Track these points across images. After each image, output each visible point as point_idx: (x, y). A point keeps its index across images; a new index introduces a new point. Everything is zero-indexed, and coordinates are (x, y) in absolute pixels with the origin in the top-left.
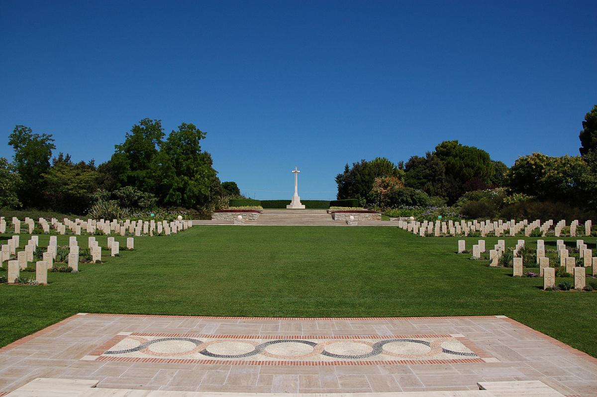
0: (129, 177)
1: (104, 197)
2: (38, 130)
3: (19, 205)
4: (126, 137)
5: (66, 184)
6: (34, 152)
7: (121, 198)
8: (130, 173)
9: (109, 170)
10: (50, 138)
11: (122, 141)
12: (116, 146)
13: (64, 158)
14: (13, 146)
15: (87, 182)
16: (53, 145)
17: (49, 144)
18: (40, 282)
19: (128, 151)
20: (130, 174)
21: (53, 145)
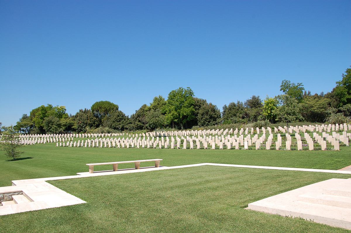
0: (347, 99)
1: (334, 112)
2: (294, 81)
3: (302, 119)
4: (342, 76)
5: (312, 107)
6: (295, 93)
7: (344, 111)
8: (348, 96)
9: (333, 97)
10: (301, 84)
11: (341, 79)
12: (337, 83)
13: (307, 93)
14: (282, 91)
15: (323, 105)
16: (303, 88)
17: (301, 87)
18: (336, 150)
19: (345, 84)
20: (348, 97)
21: (303, 88)
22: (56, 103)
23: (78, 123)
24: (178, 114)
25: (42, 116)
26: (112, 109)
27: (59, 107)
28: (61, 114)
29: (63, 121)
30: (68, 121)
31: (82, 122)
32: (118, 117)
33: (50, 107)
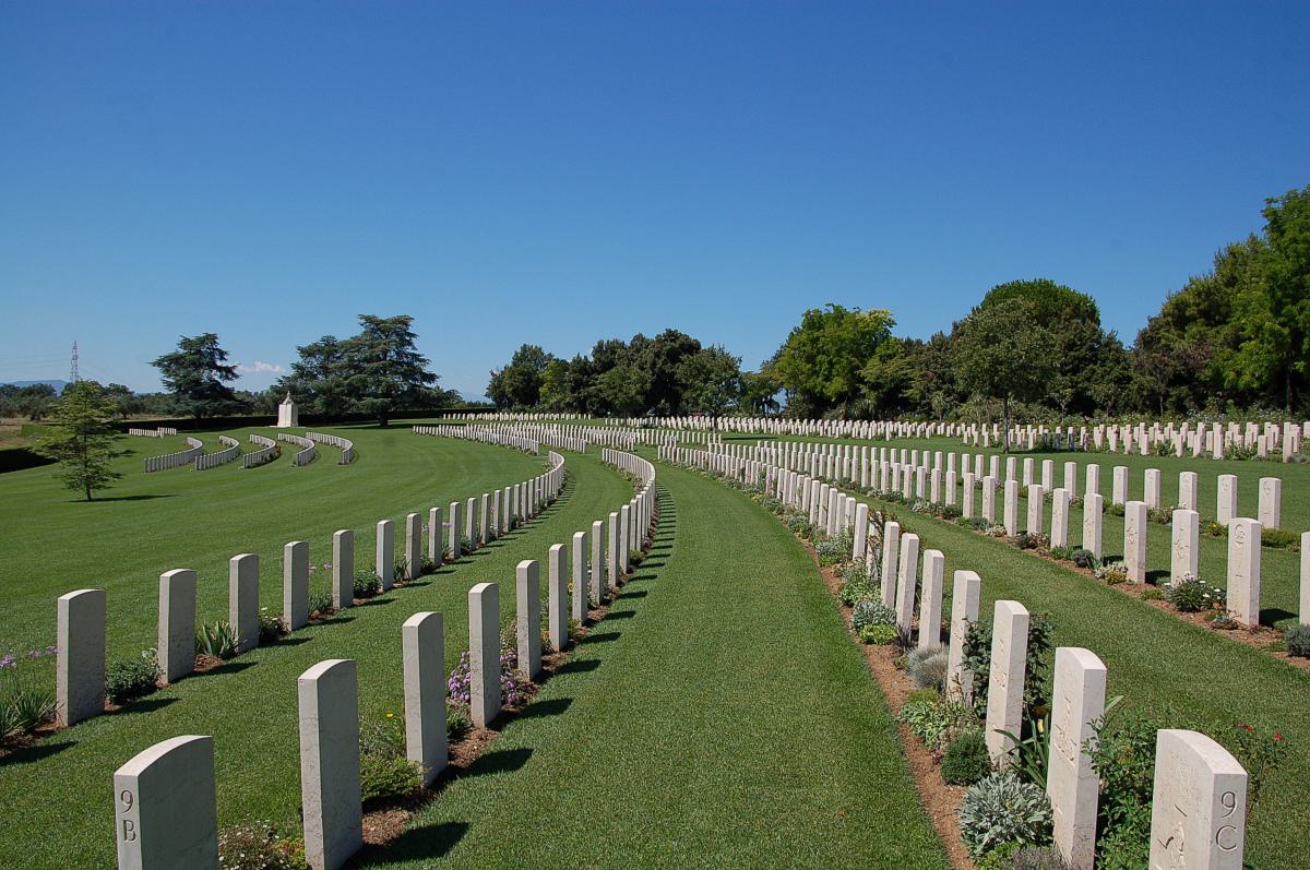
22: (862, 303)
23: (922, 376)
24: (1286, 331)
25: (808, 348)
26: (1056, 314)
27: (864, 313)
28: (870, 338)
29: (871, 369)
30: (891, 368)
31: (936, 373)
32: (1071, 350)
33: (839, 315)
